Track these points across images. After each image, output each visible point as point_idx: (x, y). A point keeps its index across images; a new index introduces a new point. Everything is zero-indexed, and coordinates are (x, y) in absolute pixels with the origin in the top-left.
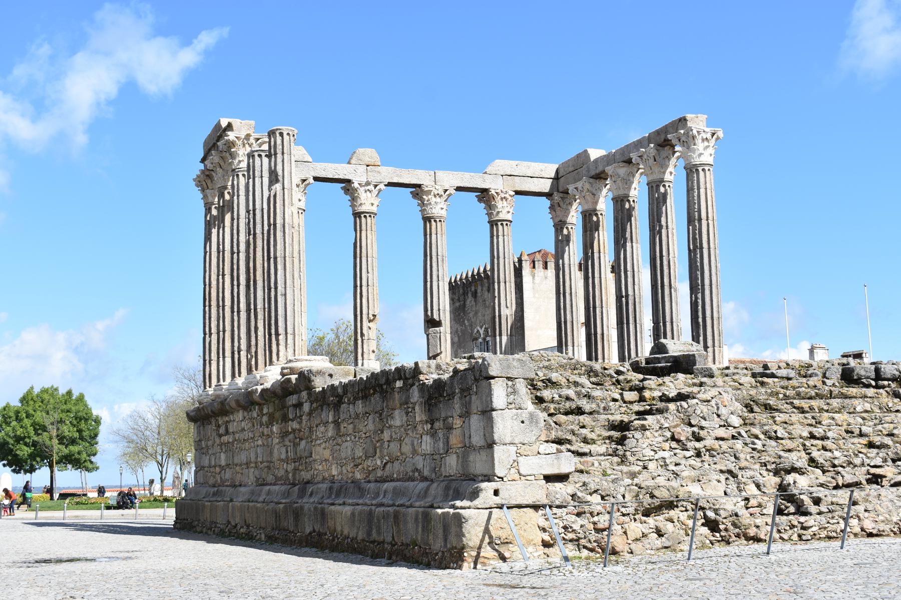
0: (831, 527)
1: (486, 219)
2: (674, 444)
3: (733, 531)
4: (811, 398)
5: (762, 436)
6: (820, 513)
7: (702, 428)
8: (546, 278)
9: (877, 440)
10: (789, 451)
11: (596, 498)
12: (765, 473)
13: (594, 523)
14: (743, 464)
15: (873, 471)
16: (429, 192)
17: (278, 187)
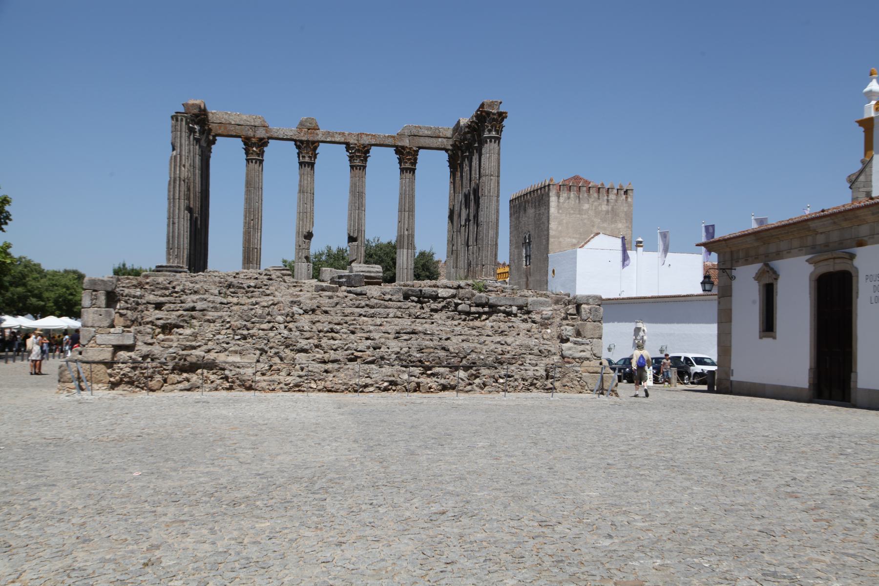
0: (305, 385)
2: (229, 331)
3: (238, 382)
4: (363, 307)
5: (294, 329)
6: (300, 377)
7: (253, 323)
8: (569, 198)
9: (372, 335)
10: (307, 339)
11: (149, 360)
12: (286, 350)
13: (143, 373)
14: (271, 345)
15: (356, 354)
16: (353, 148)
17: (174, 153)
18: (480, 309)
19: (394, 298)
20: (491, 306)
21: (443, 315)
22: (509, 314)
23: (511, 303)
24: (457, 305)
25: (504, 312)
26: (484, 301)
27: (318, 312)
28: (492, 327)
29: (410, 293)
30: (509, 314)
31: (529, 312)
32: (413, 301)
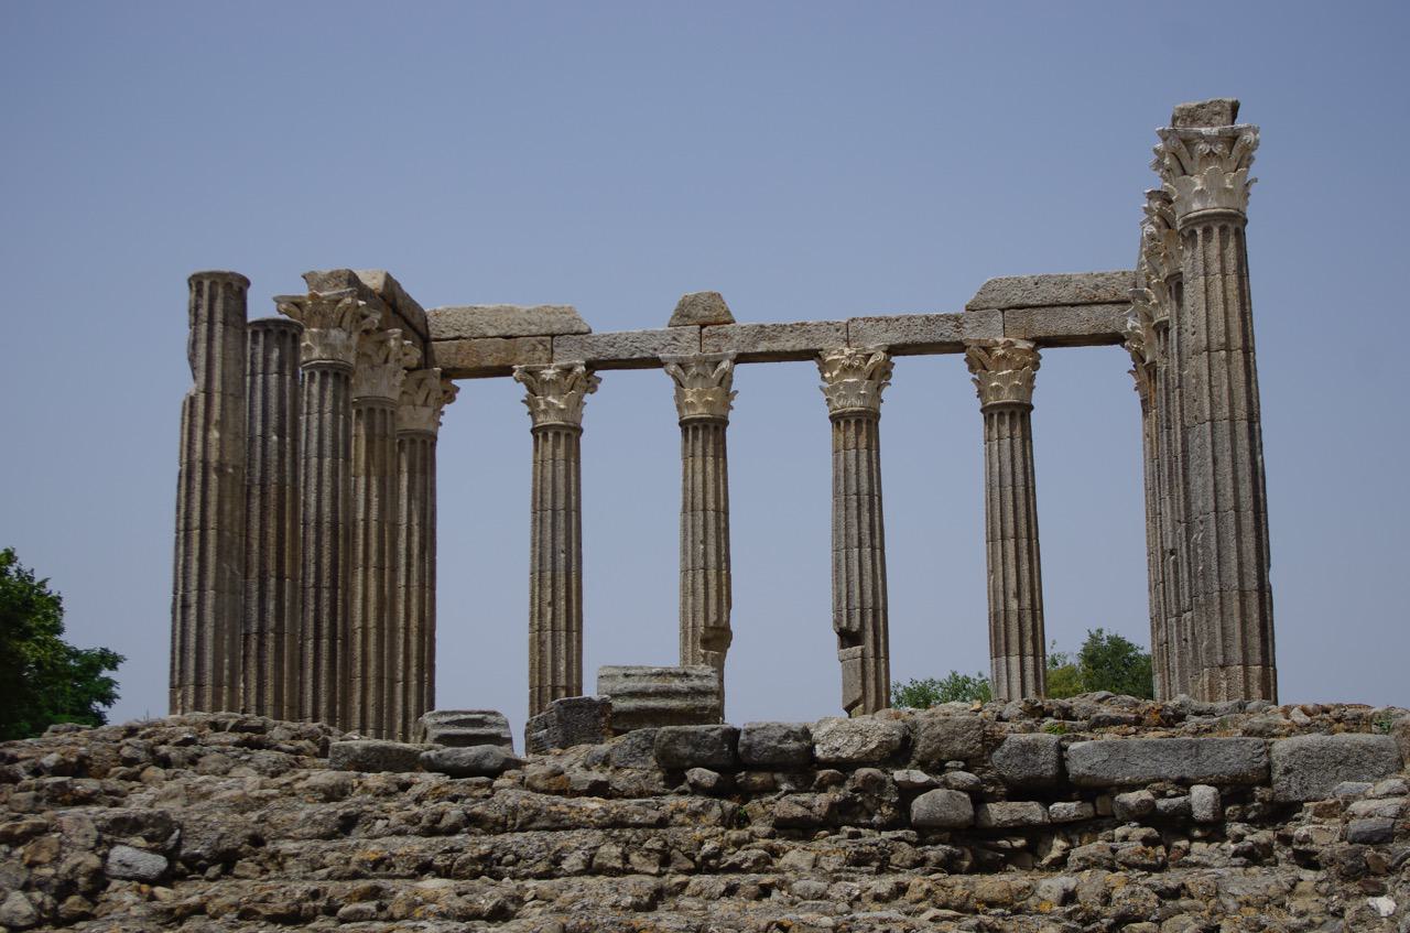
1: (978, 404)
4: (453, 830)
18: (1033, 811)
19: (620, 781)
20: (1094, 790)
21: (831, 848)
22: (1172, 825)
23: (1186, 768)
24: (909, 791)
25: (1146, 815)
26: (1046, 766)
27: (246, 866)
28: (1069, 897)
29: (684, 750)
30: (1172, 825)
31: (1282, 812)
32: (697, 789)
